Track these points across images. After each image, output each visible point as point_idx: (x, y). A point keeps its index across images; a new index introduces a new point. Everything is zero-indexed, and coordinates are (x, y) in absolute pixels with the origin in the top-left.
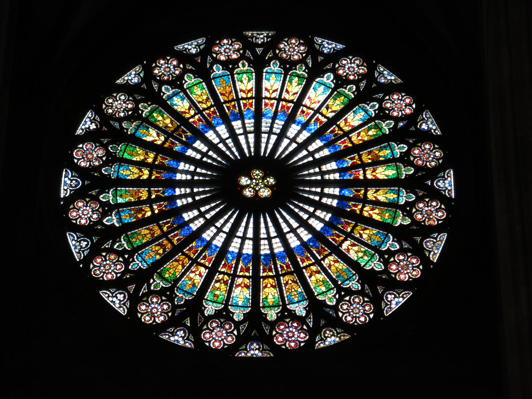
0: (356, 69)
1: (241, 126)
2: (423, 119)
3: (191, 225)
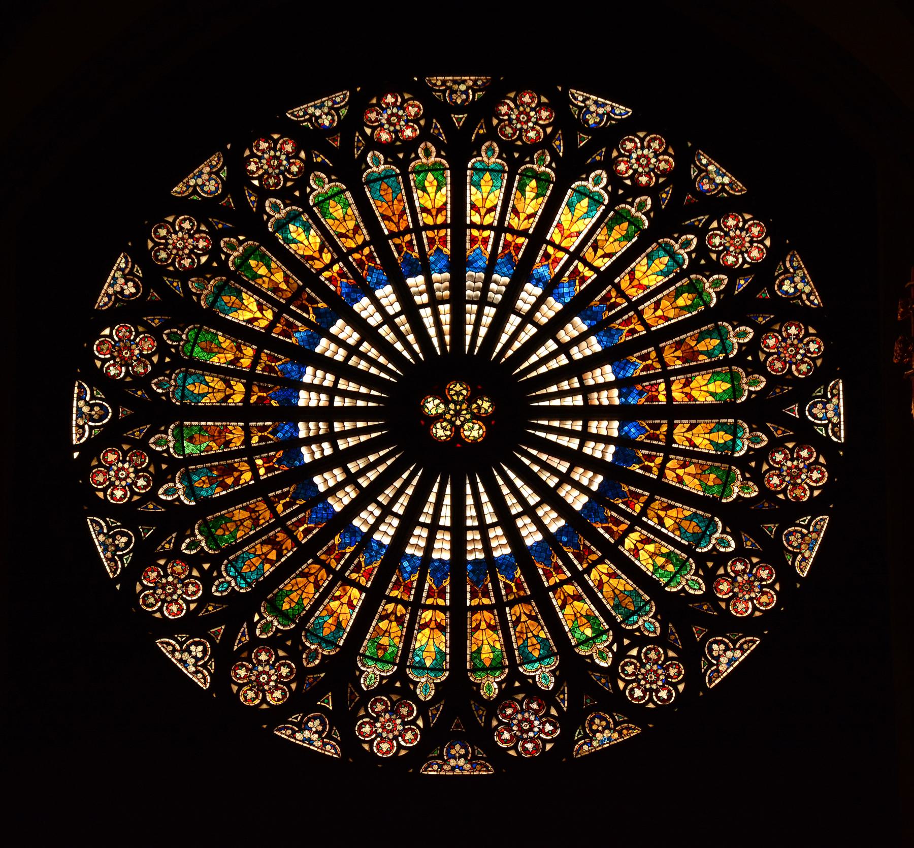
0: (653, 160)
1: (423, 287)
2: (786, 271)
3: (330, 500)
